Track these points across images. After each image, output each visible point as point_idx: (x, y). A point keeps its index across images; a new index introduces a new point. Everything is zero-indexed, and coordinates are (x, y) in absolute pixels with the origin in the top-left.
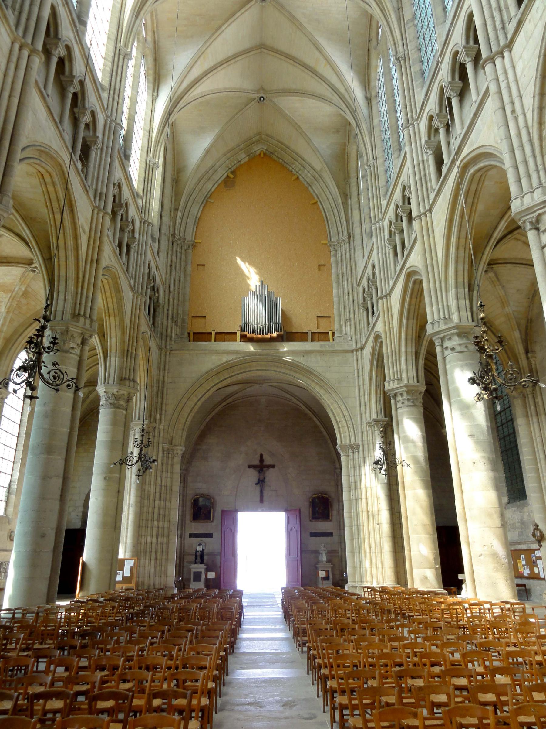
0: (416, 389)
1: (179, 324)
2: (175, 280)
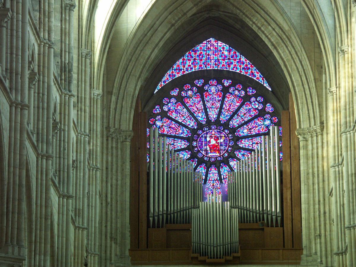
1: (118, 242)
2: (111, 186)
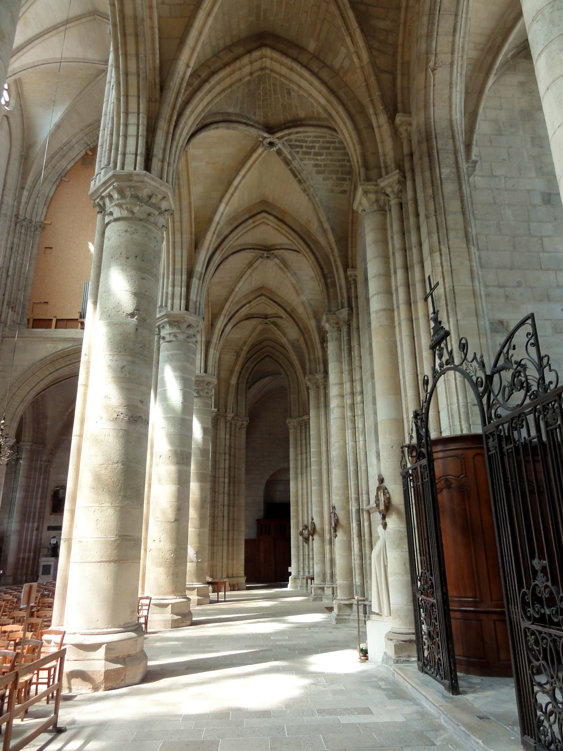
0: (202, 379)
2: (15, 263)
